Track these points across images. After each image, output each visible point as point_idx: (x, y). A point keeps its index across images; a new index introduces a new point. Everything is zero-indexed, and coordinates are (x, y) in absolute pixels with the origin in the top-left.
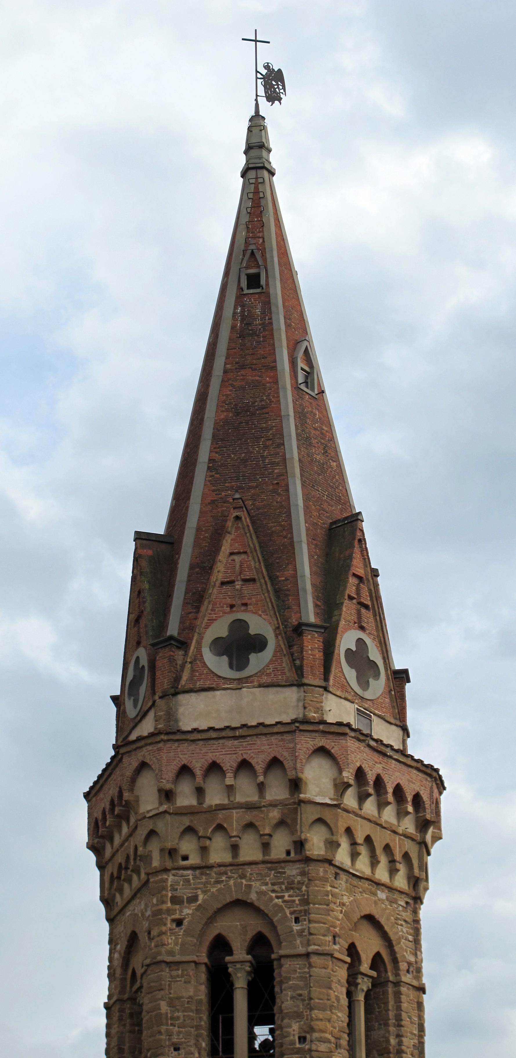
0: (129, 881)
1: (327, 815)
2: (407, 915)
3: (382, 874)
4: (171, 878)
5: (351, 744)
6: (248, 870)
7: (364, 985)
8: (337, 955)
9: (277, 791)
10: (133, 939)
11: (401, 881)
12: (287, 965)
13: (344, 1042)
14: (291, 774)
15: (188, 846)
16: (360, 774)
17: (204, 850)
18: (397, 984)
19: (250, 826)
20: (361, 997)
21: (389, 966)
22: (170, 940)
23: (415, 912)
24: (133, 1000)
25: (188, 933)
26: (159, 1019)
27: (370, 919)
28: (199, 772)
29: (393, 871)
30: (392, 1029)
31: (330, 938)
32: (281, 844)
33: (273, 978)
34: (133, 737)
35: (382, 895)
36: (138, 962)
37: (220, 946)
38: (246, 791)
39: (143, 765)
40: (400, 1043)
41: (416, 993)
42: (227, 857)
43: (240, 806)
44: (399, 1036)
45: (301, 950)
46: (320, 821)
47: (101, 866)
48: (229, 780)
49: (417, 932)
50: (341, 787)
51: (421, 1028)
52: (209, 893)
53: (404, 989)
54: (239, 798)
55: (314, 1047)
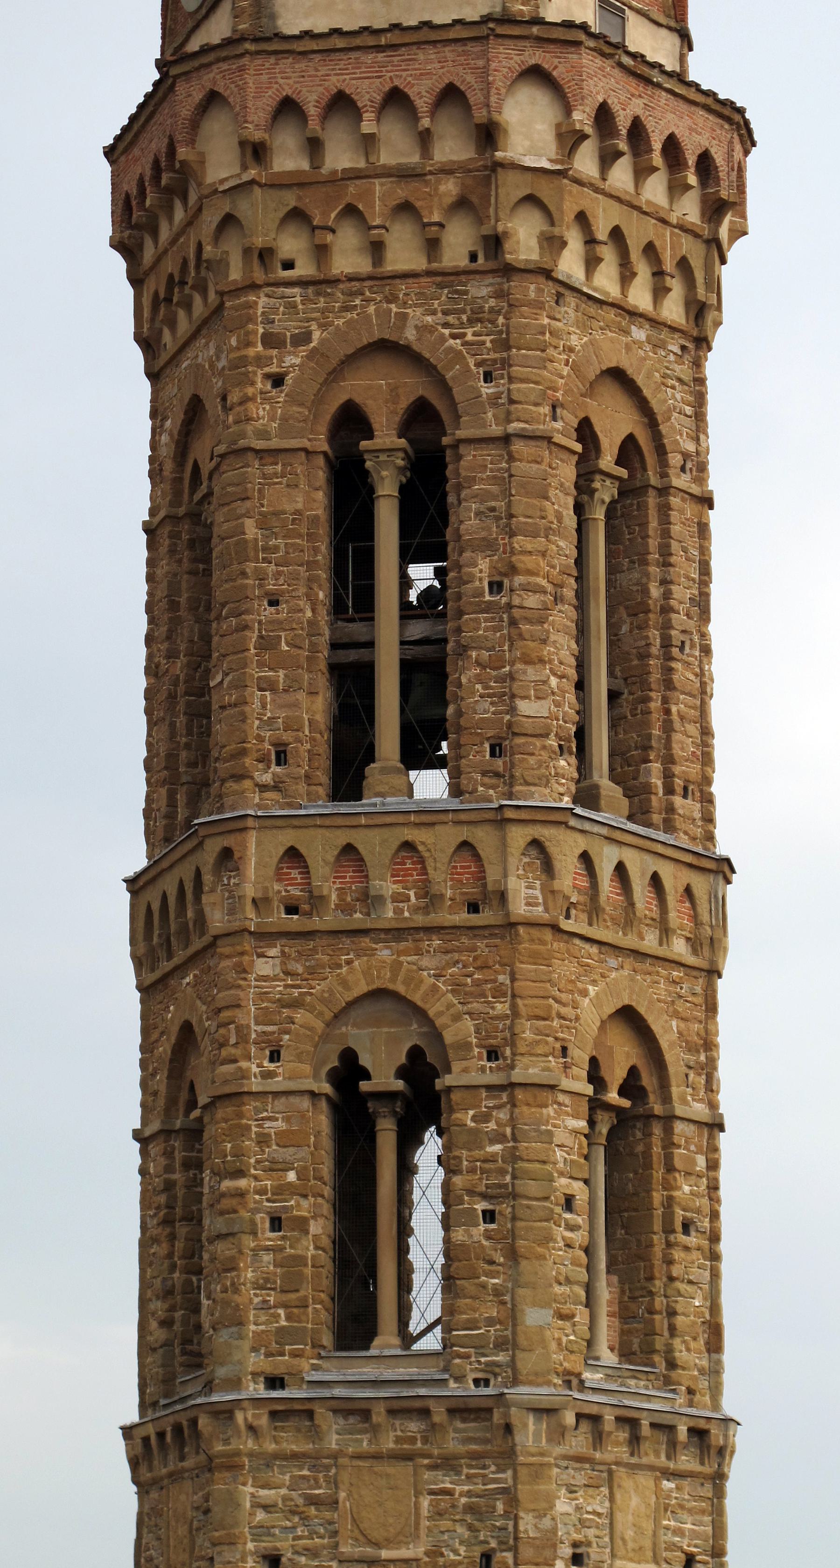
0: (188, 306)
1: (545, 190)
2: (683, 370)
3: (640, 296)
4: (262, 302)
5: (589, 61)
6: (402, 287)
7: (606, 491)
8: (558, 438)
9: (452, 147)
10: (195, 409)
11: (673, 309)
12: (469, 455)
13: (569, 593)
14: (480, 115)
15: (292, 244)
16: (604, 115)
17: (321, 252)
18: (664, 491)
19: (406, 208)
20: (600, 514)
22: (260, 411)
23: (698, 364)
24: (195, 516)
25: (292, 399)
26: (242, 550)
27: (618, 376)
28: (312, 111)
29: (659, 292)
30: (653, 570)
31: (546, 410)
32: (459, 243)
33: (445, 480)
34: (194, 46)
35: (639, 334)
36: (201, 451)
37: (352, 422)
38: (396, 147)
39: (213, 98)
41: (697, 507)
42: (362, 265)
43: (388, 173)
44: (665, 582)
45: (496, 430)
46: (531, 199)
47: (136, 279)
48: (368, 127)
49: (700, 401)
50: (570, 140)
51: (705, 570)
52: (332, 327)
53: (675, 501)
54: (386, 158)
55: (516, 601)
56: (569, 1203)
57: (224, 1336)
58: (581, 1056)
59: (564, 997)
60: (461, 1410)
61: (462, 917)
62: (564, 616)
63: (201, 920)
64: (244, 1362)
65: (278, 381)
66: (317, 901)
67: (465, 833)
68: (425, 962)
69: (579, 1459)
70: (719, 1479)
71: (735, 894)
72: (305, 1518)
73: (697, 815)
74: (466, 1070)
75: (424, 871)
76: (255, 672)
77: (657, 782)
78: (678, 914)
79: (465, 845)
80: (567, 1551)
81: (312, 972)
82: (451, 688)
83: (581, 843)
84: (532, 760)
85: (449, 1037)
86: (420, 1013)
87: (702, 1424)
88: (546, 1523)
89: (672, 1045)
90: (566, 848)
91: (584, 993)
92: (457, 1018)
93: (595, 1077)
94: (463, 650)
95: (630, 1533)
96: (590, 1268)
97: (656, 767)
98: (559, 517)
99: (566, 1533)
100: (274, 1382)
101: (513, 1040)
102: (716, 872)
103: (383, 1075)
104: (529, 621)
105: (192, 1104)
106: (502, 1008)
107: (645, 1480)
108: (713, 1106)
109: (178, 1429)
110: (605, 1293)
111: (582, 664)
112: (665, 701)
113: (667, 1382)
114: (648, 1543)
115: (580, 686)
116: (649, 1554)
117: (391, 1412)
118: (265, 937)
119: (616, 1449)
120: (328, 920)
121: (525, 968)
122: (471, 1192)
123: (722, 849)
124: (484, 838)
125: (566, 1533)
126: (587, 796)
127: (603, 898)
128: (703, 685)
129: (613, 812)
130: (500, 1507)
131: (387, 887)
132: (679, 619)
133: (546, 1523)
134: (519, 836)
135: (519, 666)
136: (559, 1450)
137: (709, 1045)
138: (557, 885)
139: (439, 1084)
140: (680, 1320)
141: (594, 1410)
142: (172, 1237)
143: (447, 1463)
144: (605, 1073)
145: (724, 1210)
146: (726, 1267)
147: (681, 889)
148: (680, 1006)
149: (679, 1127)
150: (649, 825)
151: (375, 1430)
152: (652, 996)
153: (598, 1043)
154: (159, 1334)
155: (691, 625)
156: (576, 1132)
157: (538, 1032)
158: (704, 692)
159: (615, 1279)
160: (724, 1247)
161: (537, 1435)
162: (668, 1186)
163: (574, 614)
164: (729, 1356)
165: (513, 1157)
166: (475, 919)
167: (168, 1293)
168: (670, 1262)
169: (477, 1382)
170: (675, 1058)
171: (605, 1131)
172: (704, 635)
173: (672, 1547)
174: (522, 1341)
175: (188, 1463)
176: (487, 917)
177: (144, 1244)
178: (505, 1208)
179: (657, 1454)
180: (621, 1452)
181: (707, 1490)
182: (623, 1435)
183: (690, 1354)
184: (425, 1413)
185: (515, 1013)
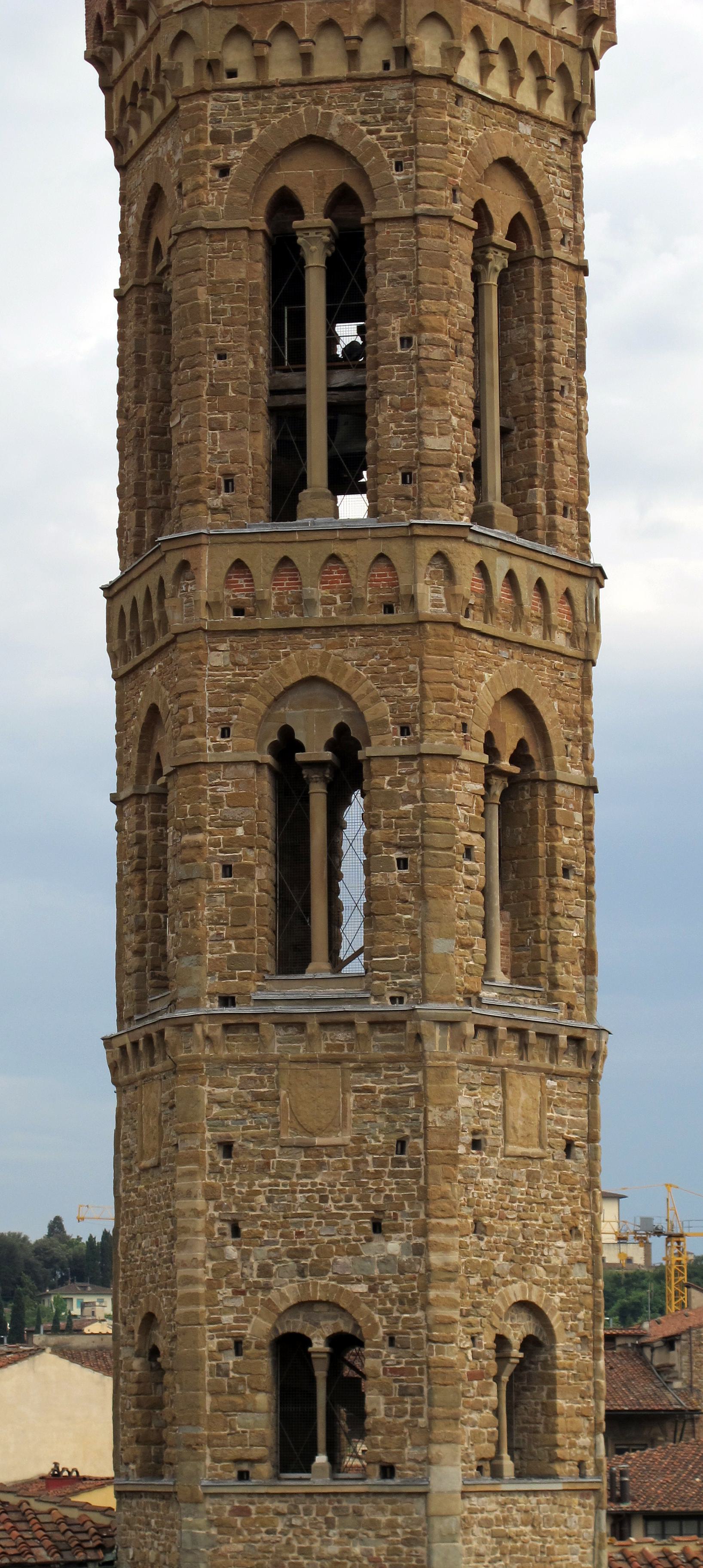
0: (149, 108)
2: (563, 159)
3: (526, 98)
4: (211, 105)
7: (498, 262)
8: (458, 218)
10: (156, 194)
11: (554, 108)
12: (384, 232)
13: (467, 346)
15: (236, 56)
17: (260, 62)
18: (547, 261)
19: (329, 24)
20: (493, 280)
21: (535, 234)
22: (210, 197)
23: (575, 154)
24: (157, 285)
25: (237, 186)
26: (195, 313)
27: (507, 164)
29: (542, 93)
30: (537, 326)
31: (448, 193)
32: (375, 52)
33: (363, 253)
35: (525, 129)
36: (163, 229)
37: (286, 204)
40: (550, 347)
41: (574, 274)
42: (294, 72)
44: (547, 337)
45: (405, 210)
47: (106, 87)
49: (577, 184)
51: (581, 327)
52: (269, 125)
53: (556, 269)
55: (423, 354)
56: (468, 852)
57: (185, 962)
58: (478, 731)
59: (464, 682)
60: (379, 1023)
61: (379, 617)
62: (463, 366)
63: (164, 621)
65: (224, 171)
66: (260, 604)
67: (381, 547)
68: (349, 654)
69: (478, 1062)
70: (593, 1078)
71: (608, 597)
72: (253, 1112)
73: (575, 531)
74: (383, 743)
75: (348, 579)
76: (207, 415)
77: (541, 503)
78: (559, 614)
79: (381, 556)
80: (468, 1138)
81: (255, 662)
82: (369, 427)
83: (478, 555)
84: (437, 486)
85: (369, 716)
86: (345, 696)
87: (579, 1034)
88: (450, 1115)
89: (554, 722)
90: (464, 559)
91: (481, 679)
92: (375, 700)
93: (490, 748)
94: (379, 394)
95: (519, 1123)
96: (487, 906)
97: (540, 491)
98: (459, 283)
100: (227, 1000)
101: (421, 717)
102: (590, 578)
103: (315, 748)
104: (434, 370)
105: (158, 772)
106: (412, 691)
107: (532, 1079)
108: (588, 771)
109: (148, 1039)
110: (498, 926)
111: (478, 405)
112: (548, 436)
113: (551, 999)
114: (534, 1131)
115: (477, 424)
116: (536, 1140)
117: (323, 1025)
118: (216, 634)
119: (508, 1054)
120: (268, 620)
121: (432, 658)
122: (388, 844)
123: (596, 558)
124: (396, 550)
126: (483, 516)
127: (496, 601)
128: (580, 422)
129: (505, 528)
130: (412, 1102)
131: (318, 592)
132: (559, 368)
133: (450, 1115)
134: (426, 549)
135: (426, 408)
136: (461, 1055)
137: (585, 721)
138: (458, 589)
139: (361, 755)
140: (561, 948)
141: (489, 1022)
142: (143, 882)
143: (369, 1067)
144: (498, 745)
145: (597, 858)
146: (598, 904)
147: (562, 592)
148: (561, 689)
149: (560, 789)
150: (534, 539)
151: (310, 1039)
152: (537, 681)
153: (492, 720)
154: (133, 962)
155: (570, 373)
156: (474, 793)
157: (442, 711)
158: (580, 429)
159: (507, 914)
160: (597, 888)
161: (443, 1042)
162: (551, 838)
163: (471, 364)
164: (600, 979)
165: (422, 814)
166: (390, 618)
167: (141, 927)
168: (553, 901)
169: (393, 999)
170: (557, 732)
171: (499, 793)
172: (580, 381)
173: (555, 1134)
174: (430, 965)
175: (156, 1068)
176: (400, 616)
177: (119, 888)
178: (415, 857)
179: (542, 1058)
180: (513, 1056)
181: (584, 1088)
182: (513, 1043)
183: (569, 976)
184: (351, 1025)
185: (424, 696)
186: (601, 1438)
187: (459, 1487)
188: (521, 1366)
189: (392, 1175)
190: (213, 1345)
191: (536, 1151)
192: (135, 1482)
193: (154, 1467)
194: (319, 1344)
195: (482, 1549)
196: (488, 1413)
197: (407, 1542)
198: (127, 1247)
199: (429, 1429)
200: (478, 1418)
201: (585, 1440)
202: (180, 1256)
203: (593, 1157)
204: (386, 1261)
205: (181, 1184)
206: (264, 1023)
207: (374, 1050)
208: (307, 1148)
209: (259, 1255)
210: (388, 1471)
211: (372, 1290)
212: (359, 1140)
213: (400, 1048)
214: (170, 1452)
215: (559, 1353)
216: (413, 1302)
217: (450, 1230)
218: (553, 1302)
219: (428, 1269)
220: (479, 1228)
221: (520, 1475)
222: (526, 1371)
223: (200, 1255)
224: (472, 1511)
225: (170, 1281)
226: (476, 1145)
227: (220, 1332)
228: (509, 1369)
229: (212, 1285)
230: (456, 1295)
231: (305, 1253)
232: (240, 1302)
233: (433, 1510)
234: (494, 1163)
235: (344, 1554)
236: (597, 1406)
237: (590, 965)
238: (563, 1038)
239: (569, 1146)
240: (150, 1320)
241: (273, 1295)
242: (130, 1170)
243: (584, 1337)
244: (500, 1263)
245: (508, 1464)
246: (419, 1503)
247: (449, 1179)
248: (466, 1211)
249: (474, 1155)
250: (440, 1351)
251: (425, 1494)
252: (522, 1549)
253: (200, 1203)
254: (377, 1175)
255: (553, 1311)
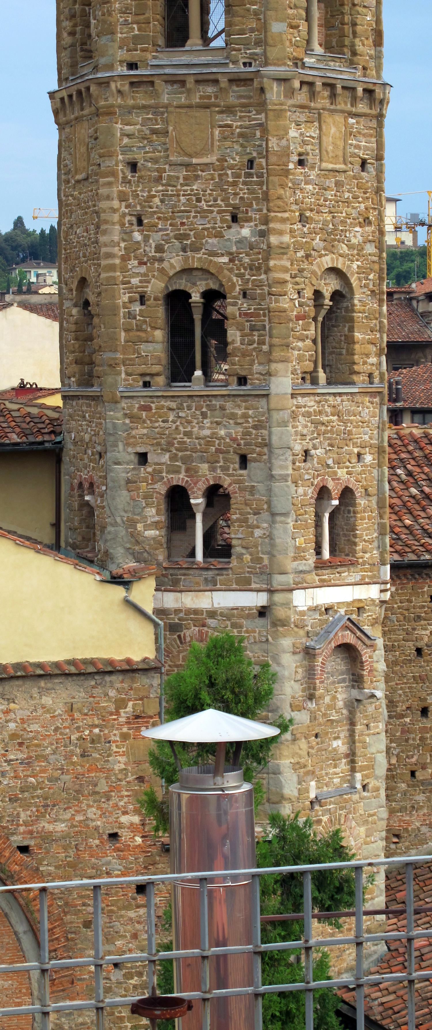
57: (104, 40)
60: (235, 80)
64: (114, 54)
69: (302, 107)
70: (380, 117)
72: (150, 142)
80: (295, 158)
87: (371, 87)
88: (284, 142)
95: (330, 148)
99: (295, 148)
100: (132, 66)
107: (339, 118)
109: (79, 93)
110: (316, 13)
113: (352, 64)
114: (340, 153)
116: (341, 159)
117: (197, 82)
119: (323, 101)
125: (295, 148)
130: (258, 134)
133: (284, 142)
136: (290, 102)
140: (359, 28)
141: (310, 79)
143: (229, 110)
151: (189, 91)
154: (68, 40)
159: (322, 5)
161: (278, 93)
164: (386, 49)
167: (73, 16)
169: (245, 64)
173: (354, 155)
174: (270, 41)
179: (346, 104)
181: (374, 124)
182: (326, 93)
183: (364, 48)
184: (216, 81)
186: (384, 358)
187: (290, 391)
188: (331, 311)
189: (245, 183)
190: (126, 298)
191: (341, 167)
192: (75, 389)
193: (87, 379)
194: (196, 297)
195: (305, 431)
196: (308, 342)
197: (255, 427)
198: (67, 234)
199: (270, 352)
200: (302, 346)
201: (373, 360)
202: (103, 239)
203: (380, 171)
204: (240, 241)
205: (103, 191)
206: (157, 81)
207: (232, 99)
208: (187, 166)
209: (155, 238)
210: (242, 381)
211: (231, 261)
212: (222, 160)
213: (250, 97)
214: (98, 370)
215: (356, 302)
216: (259, 269)
217: (284, 220)
218: (353, 268)
219: (269, 246)
220: (303, 219)
221: (330, 382)
222: (334, 314)
223: (116, 238)
224: (298, 407)
225: (96, 256)
226: (301, 163)
227: (130, 290)
228: (323, 313)
229: (125, 259)
230: (288, 264)
231: (186, 236)
232: (143, 269)
233: (272, 406)
234: (313, 175)
235: (214, 435)
236: (382, 337)
237: (378, 40)
238: (360, 90)
239: (364, 164)
240: (83, 282)
241: (165, 265)
242: (68, 182)
243: (372, 291)
244: (317, 242)
245: (322, 376)
246: (263, 402)
247: (282, 186)
248: (294, 207)
249: (300, 170)
250: (277, 301)
251: (267, 396)
252: (331, 431)
253: (116, 203)
254: (235, 184)
255: (353, 274)
